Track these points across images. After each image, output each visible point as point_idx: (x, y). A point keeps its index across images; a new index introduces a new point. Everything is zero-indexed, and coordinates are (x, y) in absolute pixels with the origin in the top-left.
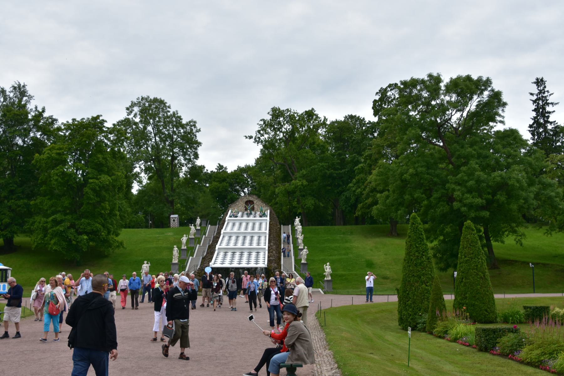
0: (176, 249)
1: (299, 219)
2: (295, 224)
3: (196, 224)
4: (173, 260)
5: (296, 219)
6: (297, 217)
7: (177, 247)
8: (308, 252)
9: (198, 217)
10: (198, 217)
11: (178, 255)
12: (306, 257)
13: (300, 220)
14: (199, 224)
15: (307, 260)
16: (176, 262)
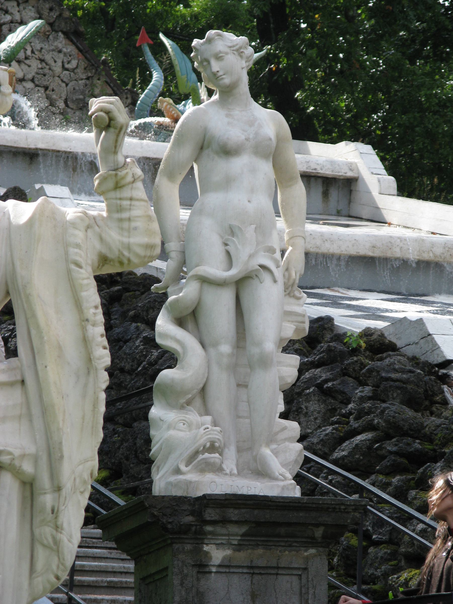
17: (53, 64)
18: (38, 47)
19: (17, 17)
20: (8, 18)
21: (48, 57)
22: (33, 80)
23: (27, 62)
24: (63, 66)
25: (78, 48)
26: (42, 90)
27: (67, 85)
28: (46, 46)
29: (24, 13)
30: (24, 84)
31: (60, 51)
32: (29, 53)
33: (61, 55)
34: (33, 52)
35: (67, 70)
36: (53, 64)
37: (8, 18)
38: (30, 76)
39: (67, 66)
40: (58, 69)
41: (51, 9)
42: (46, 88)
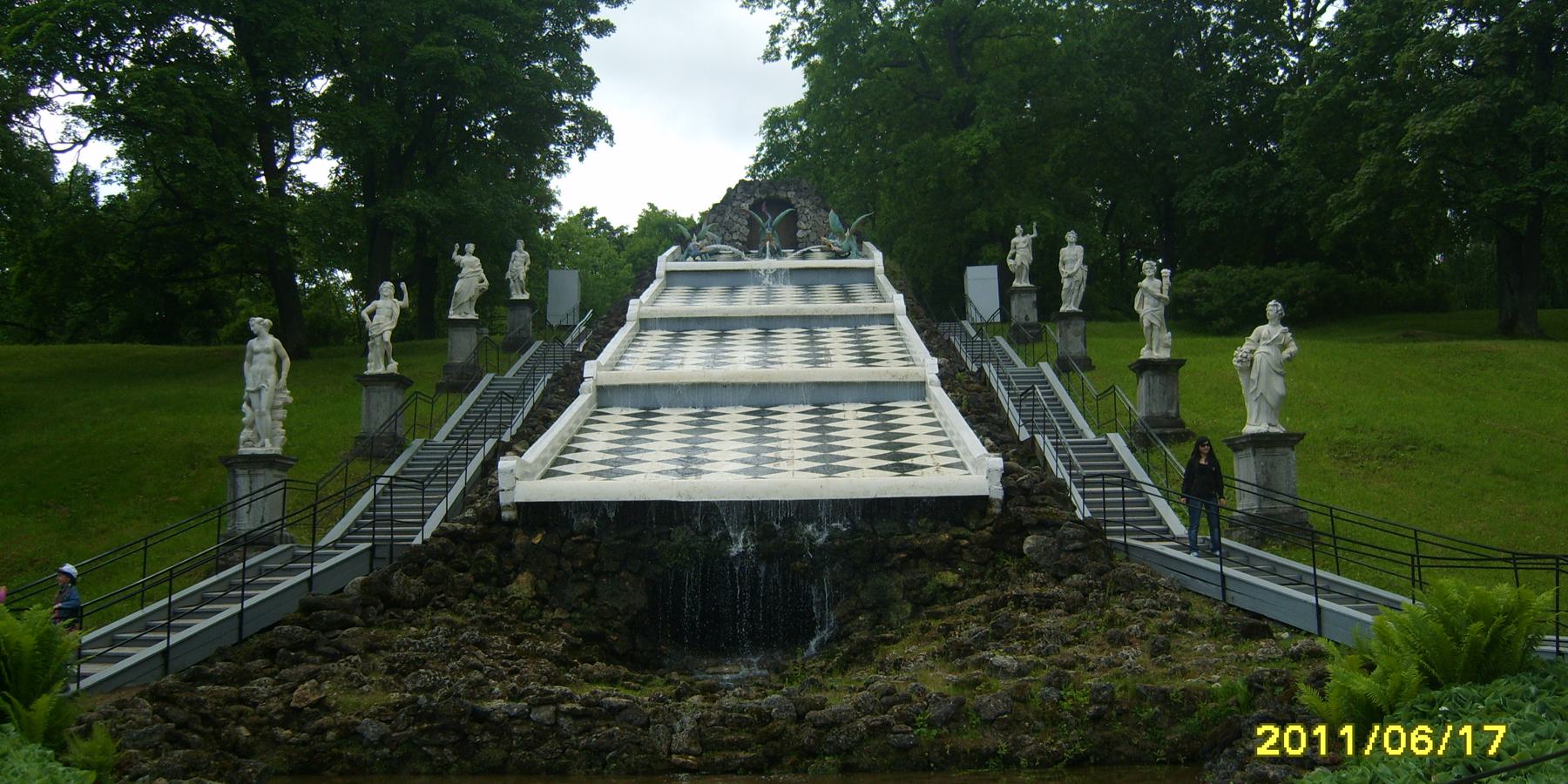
0: (271, 341)
1: (1029, 237)
2: (1010, 262)
3: (508, 275)
4: (246, 434)
5: (1014, 240)
6: (1019, 229)
7: (273, 331)
8: (1293, 348)
9: (520, 243)
10: (520, 243)
11: (286, 396)
12: (1278, 386)
13: (1033, 239)
14: (523, 276)
15: (1282, 407)
16: (270, 447)
40: (821, 223)
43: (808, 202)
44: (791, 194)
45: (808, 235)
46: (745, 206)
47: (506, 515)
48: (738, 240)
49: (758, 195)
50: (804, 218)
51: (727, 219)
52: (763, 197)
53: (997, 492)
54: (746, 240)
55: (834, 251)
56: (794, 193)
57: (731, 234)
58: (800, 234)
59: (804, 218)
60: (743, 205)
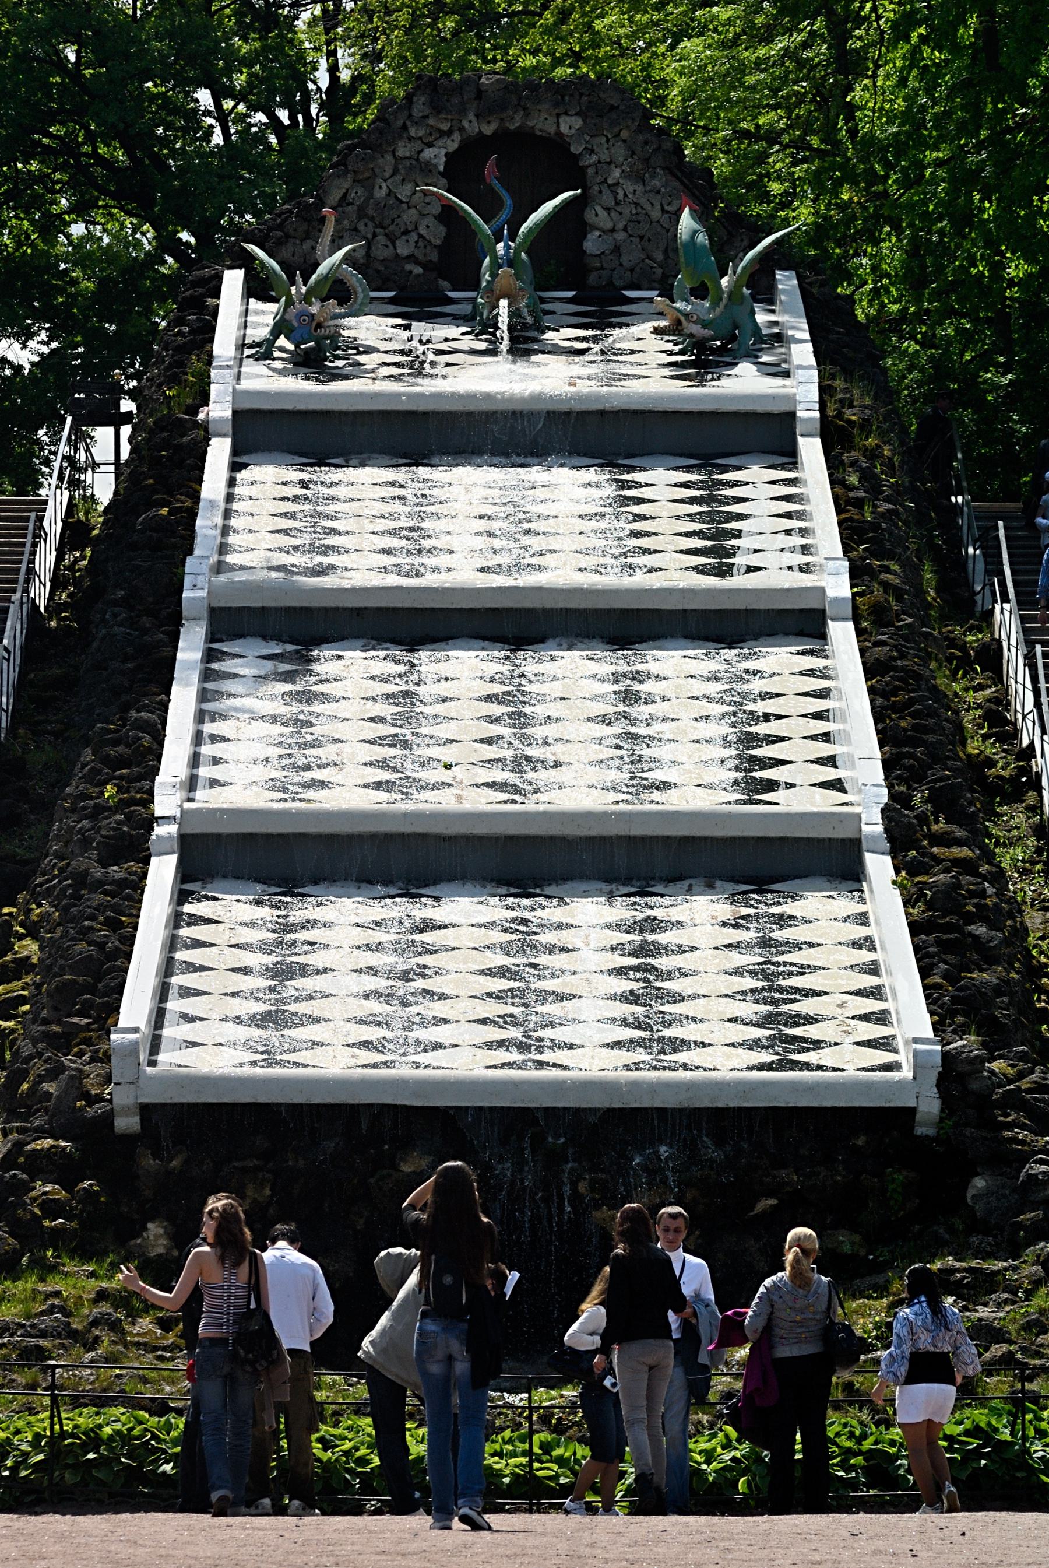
17: (648, 207)
18: (631, 189)
19: (605, 157)
20: (595, 158)
21: (643, 201)
22: (625, 229)
23: (619, 209)
24: (663, 209)
25: (682, 183)
26: (636, 240)
27: (668, 231)
28: (640, 188)
29: (613, 151)
30: (615, 235)
31: (658, 192)
32: (621, 197)
33: (659, 197)
34: (625, 195)
35: (668, 212)
36: (648, 207)
37: (595, 158)
38: (620, 226)
39: (666, 208)
40: (656, 214)
41: (646, 143)
42: (641, 238)
43: (619, 152)
44: (569, 125)
45: (617, 250)
46: (436, 155)
47: (127, 1123)
48: (411, 258)
49: (472, 125)
50: (607, 199)
51: (380, 193)
52: (488, 130)
53: (930, 1106)
54: (434, 256)
55: (691, 335)
56: (578, 122)
57: (392, 239)
58: (592, 244)
59: (607, 199)
60: (428, 153)
